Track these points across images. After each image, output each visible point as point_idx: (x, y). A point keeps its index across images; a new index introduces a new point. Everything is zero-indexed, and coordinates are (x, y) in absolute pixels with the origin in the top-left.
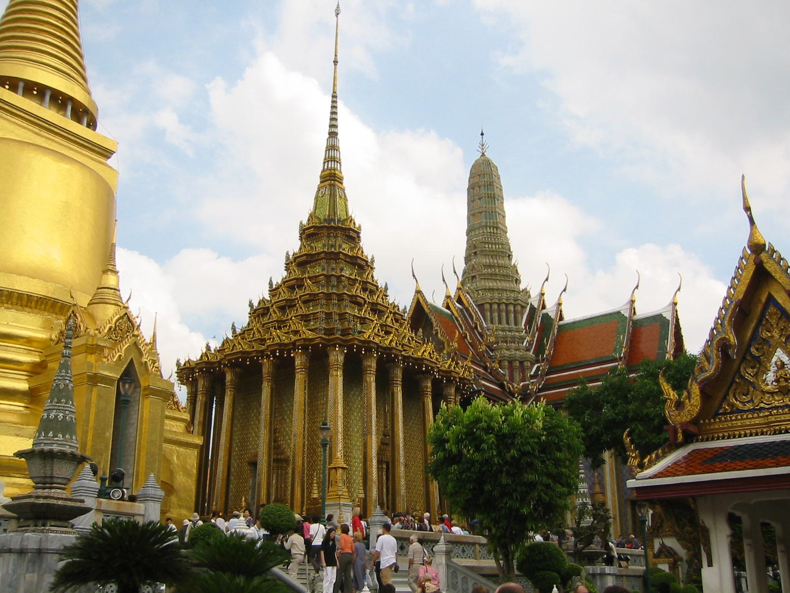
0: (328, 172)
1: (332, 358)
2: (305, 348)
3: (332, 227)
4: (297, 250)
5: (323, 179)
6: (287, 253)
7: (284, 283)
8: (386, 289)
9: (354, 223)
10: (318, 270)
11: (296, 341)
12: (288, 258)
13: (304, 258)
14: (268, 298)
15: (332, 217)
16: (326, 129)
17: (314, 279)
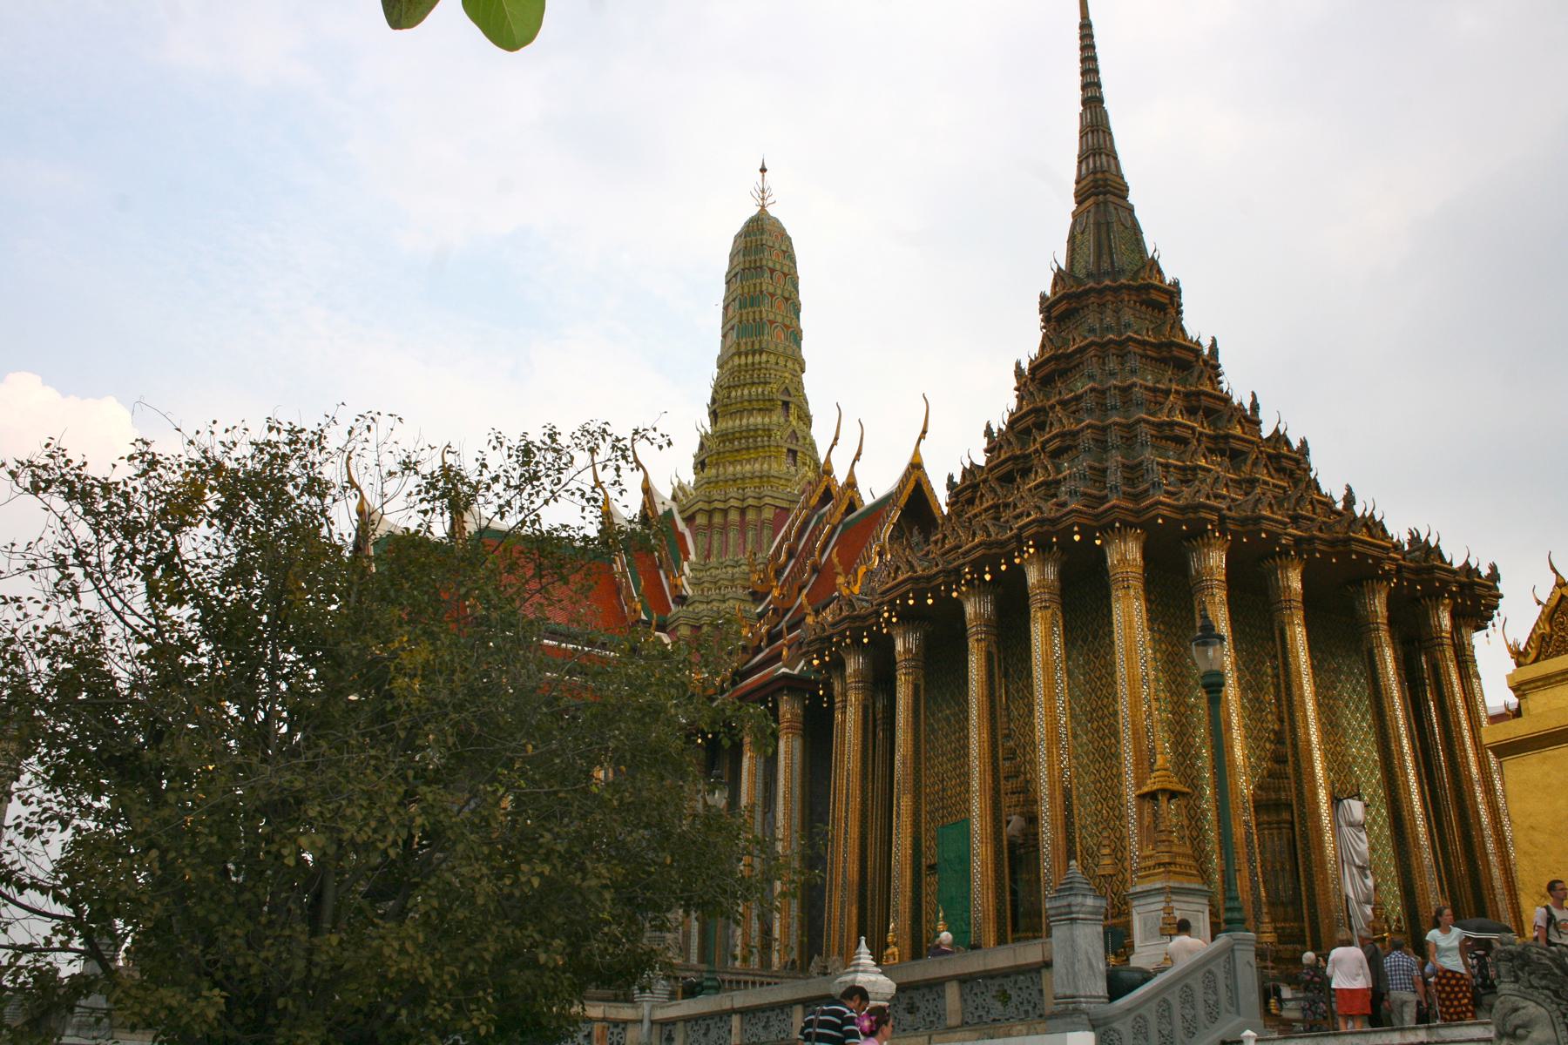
0: (1090, 178)
1: (1112, 558)
2: (1043, 547)
3: (1107, 288)
4: (1035, 350)
5: (1081, 197)
6: (1018, 365)
7: (1014, 421)
8: (1255, 406)
9: (1159, 271)
10: (1082, 386)
11: (1021, 529)
12: (1019, 372)
13: (1052, 365)
14: (981, 460)
15: (1106, 266)
16: (1077, 95)
17: (1072, 405)
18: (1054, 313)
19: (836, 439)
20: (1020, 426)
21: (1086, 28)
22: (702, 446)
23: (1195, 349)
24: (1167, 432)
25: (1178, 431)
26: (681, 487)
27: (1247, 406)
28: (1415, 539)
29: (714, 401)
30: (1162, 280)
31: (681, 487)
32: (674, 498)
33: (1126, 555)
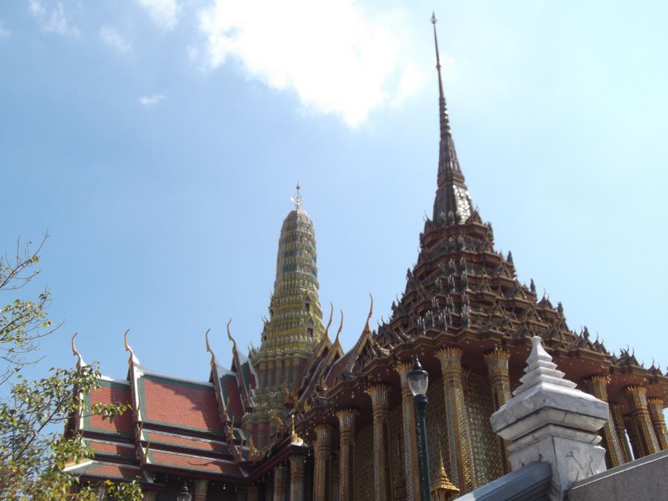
8: (533, 287)
9: (479, 218)
13: (422, 271)
18: (426, 243)
19: (330, 321)
20: (407, 303)
21: (442, 101)
22: (265, 329)
23: (499, 258)
24: (480, 299)
25: (486, 298)
26: (253, 351)
27: (528, 286)
28: (625, 355)
29: (272, 305)
30: (480, 222)
31: (253, 351)
32: (250, 356)
33: (450, 360)
